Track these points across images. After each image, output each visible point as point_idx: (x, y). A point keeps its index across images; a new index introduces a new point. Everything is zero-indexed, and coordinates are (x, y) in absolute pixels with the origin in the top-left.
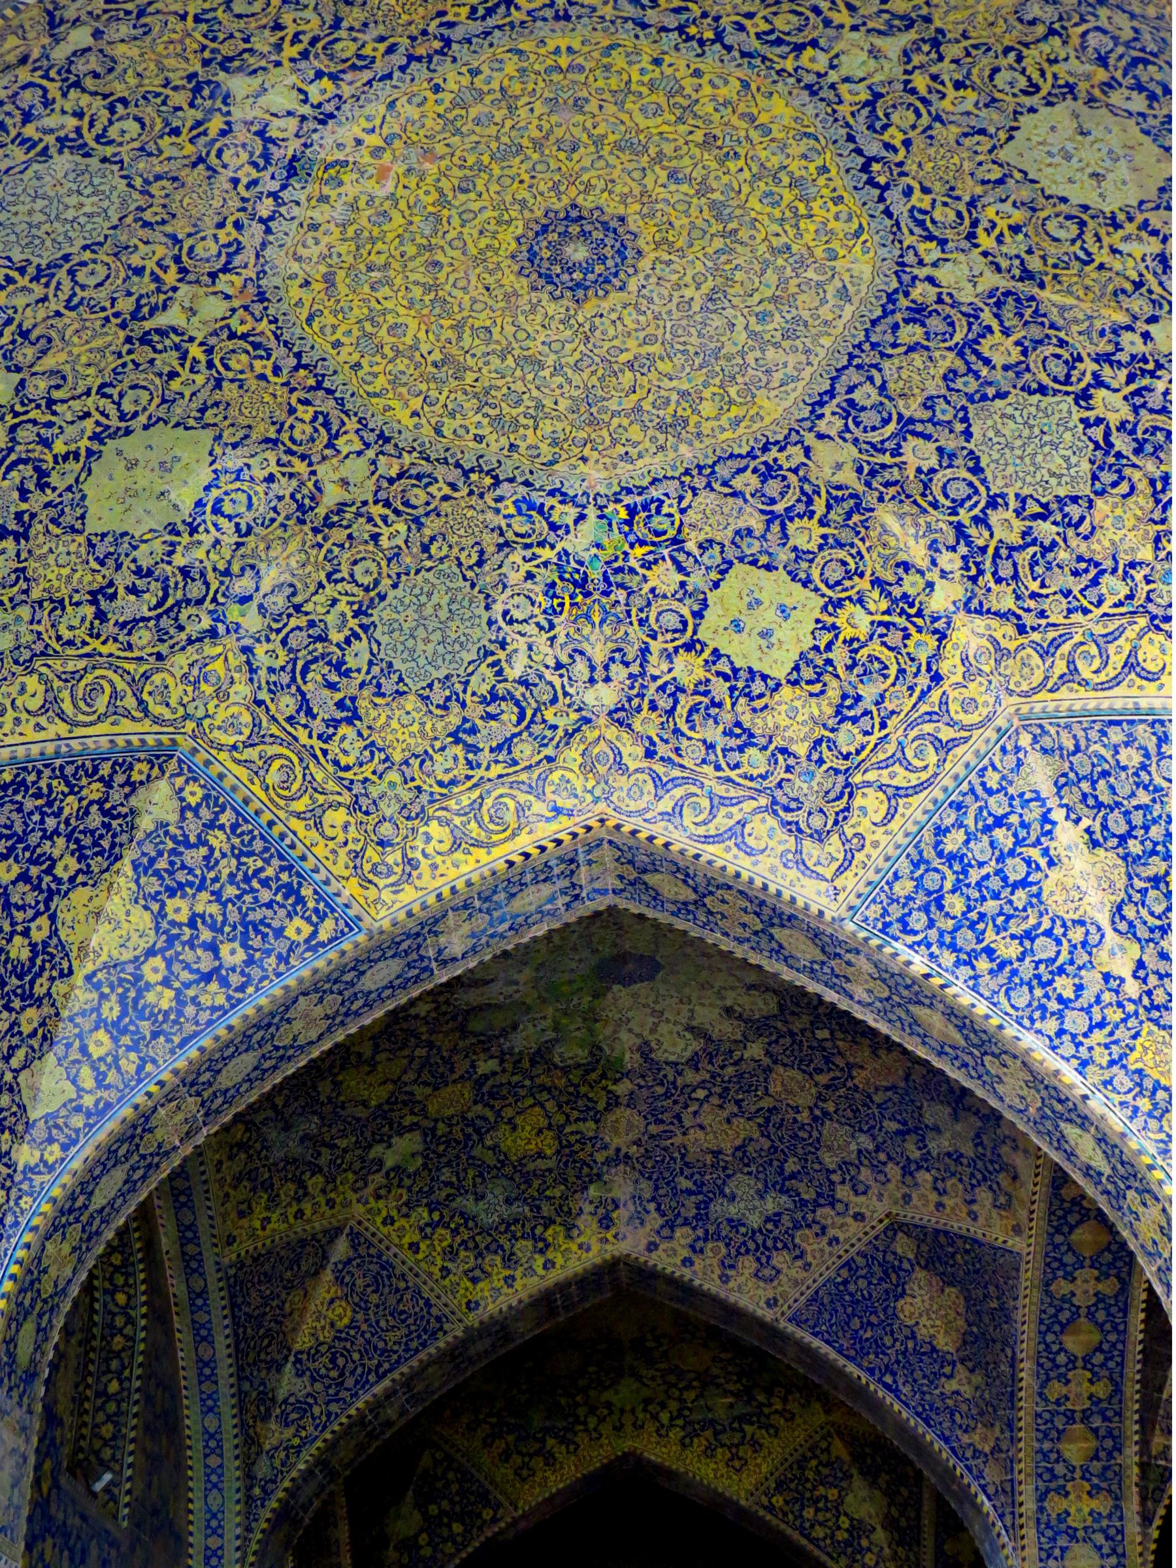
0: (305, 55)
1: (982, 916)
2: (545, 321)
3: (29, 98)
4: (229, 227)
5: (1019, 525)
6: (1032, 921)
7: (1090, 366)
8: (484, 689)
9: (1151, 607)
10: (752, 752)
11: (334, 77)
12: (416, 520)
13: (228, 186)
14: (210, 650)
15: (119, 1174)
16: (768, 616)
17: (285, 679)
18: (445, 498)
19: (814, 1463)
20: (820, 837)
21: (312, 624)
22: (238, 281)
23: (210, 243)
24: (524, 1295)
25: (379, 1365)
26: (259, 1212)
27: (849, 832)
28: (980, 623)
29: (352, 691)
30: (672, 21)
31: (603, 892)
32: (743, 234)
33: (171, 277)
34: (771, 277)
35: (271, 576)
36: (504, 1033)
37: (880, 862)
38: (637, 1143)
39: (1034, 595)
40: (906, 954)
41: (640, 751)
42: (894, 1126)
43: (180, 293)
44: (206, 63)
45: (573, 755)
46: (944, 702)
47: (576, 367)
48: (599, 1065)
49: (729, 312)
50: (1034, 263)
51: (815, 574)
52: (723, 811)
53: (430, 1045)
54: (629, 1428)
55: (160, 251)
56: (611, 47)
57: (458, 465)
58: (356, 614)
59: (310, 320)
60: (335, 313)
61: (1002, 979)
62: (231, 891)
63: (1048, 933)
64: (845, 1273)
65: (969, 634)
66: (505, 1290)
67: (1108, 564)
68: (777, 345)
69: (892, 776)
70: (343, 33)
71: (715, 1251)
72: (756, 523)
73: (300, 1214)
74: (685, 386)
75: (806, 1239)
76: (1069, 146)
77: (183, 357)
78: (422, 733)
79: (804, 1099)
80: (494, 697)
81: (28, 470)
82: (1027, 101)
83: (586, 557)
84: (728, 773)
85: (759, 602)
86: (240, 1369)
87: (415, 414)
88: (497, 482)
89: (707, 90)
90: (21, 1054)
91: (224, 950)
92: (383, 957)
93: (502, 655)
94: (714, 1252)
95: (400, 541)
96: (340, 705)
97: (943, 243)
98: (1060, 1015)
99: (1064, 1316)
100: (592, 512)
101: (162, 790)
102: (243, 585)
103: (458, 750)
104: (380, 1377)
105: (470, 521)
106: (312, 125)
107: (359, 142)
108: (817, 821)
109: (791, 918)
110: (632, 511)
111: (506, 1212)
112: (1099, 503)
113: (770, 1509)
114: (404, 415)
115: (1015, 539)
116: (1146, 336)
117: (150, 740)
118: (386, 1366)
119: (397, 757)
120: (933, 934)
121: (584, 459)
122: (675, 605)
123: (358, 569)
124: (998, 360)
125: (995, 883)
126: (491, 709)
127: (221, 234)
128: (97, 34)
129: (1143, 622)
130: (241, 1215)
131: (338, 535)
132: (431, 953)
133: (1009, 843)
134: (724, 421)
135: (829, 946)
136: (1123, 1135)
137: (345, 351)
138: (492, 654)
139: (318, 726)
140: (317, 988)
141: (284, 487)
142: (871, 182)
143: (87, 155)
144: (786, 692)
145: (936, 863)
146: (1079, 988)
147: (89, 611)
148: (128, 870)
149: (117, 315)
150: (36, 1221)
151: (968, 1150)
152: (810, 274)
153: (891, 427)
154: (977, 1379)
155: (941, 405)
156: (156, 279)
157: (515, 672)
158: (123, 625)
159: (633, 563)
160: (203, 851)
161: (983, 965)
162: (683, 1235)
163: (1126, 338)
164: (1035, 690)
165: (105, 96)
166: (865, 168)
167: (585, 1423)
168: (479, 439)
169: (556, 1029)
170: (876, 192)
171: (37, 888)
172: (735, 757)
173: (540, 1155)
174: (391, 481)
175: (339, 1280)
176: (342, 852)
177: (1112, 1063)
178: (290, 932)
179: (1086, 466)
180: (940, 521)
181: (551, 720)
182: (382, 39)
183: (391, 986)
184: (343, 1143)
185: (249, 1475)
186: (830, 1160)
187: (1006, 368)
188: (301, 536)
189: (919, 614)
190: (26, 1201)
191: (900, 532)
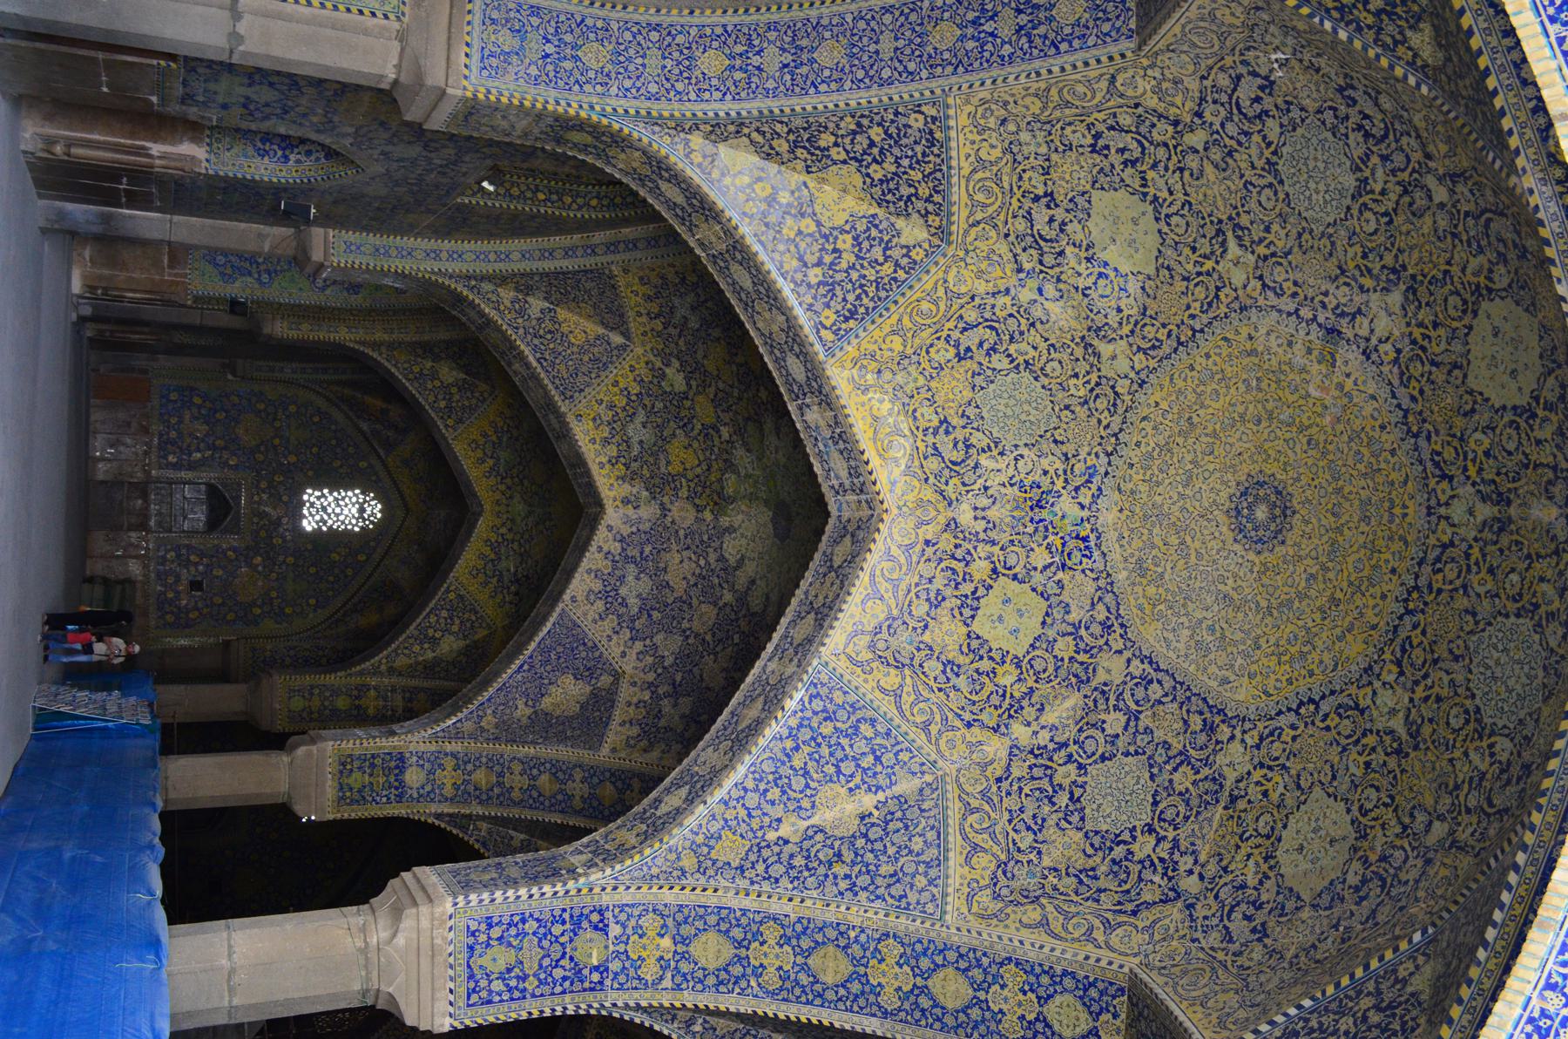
0: (1414, 342)
1: (819, 745)
2: (1217, 490)
3: (1399, 159)
4: (1294, 289)
5: (1066, 783)
6: (815, 776)
7: (1171, 834)
8: (973, 441)
9: (1012, 863)
10: (926, 606)
11: (1396, 361)
12: (1086, 402)
13: (1323, 289)
14: (1010, 267)
15: (680, 200)
16: (1012, 622)
17: (987, 315)
18: (1099, 421)
20: (872, 647)
21: (1022, 333)
22: (1255, 294)
23: (1284, 276)
24: (584, 449)
26: (642, 290)
27: (874, 665)
28: (1004, 754)
29: (977, 358)
30: (1422, 582)
31: (840, 510)
32: (1269, 620)
33: (1262, 250)
34: (1238, 636)
35: (1055, 309)
36: (745, 444)
37: (855, 683)
38: (673, 522)
39: (1020, 789)
40: (797, 696)
41: (929, 537)
42: (678, 678)
43: (1250, 256)
44: (1413, 277)
45: (928, 494)
46: (953, 729)
47: (1183, 509)
48: (721, 502)
49: (1216, 608)
50: (1241, 804)
51: (1037, 652)
52: (890, 587)
53: (740, 399)
55: (1280, 244)
56: (1406, 543)
57: (1121, 430)
58: (1026, 362)
59: (1225, 339)
60: (1229, 355)
61: (780, 755)
62: (855, 275)
63: (807, 786)
64: (590, 644)
65: (996, 748)
67: (1040, 837)
68: (1192, 637)
69: (908, 694)
70: (1427, 368)
71: (606, 567)
72: (1074, 617)
73: (639, 314)
74: (1167, 577)
75: (610, 622)
76: (1323, 833)
77: (1205, 257)
78: (948, 401)
79: (696, 625)
80: (968, 447)
81: (1137, 154)
82: (1355, 808)
83: (1056, 509)
84: (914, 591)
85: (1021, 616)
86: (547, 275)
87: (1157, 404)
88: (1108, 455)
89: (1371, 602)
90: (760, 139)
91: (818, 270)
92: (807, 370)
93: (995, 452)
94: (604, 565)
95: (1073, 391)
96: (968, 349)
97: (1258, 747)
98: (756, 790)
99: (560, 775)
100: (1085, 513)
101: (921, 234)
102: (1050, 290)
103: (936, 423)
104: (538, 360)
105: (1083, 437)
106: (1363, 345)
107: (1348, 375)
108: (881, 645)
109: (821, 626)
110: (1085, 539)
111: (635, 439)
112: (1081, 834)
113: (448, 591)
114: (1157, 397)
115: (1057, 779)
116: (1191, 872)
117: (954, 228)
119: (933, 384)
120: (809, 714)
121: (1121, 511)
122: (1022, 563)
123: (1055, 364)
124: (1177, 777)
125: (839, 754)
126: (960, 445)
127: (1290, 284)
128: (1442, 206)
129: (1003, 857)
130: (641, 279)
131: (1079, 352)
132: (808, 401)
133: (864, 765)
134: (1141, 600)
135: (804, 648)
136: (681, 825)
137: (1203, 361)
138: (995, 446)
139: (956, 335)
140: (791, 327)
141: (1113, 319)
142: (1301, 704)
143: (1353, 197)
144: (964, 630)
145: (853, 718)
146: (773, 803)
147: (1040, 192)
148: (872, 211)
149: (1238, 214)
150: (655, 146)
151: (663, 723)
152: (1240, 661)
153: (1134, 707)
154: (525, 721)
155: (1147, 738)
156: (1261, 241)
157: (984, 461)
158: (1029, 213)
159: (1051, 538)
160: (881, 259)
161: (789, 744)
162: (616, 547)
163: (1190, 860)
164: (960, 786)
165: (1395, 210)
166: (1311, 701)
168: (1138, 444)
169: (748, 476)
170: (1294, 707)
171: (865, 153)
172: (923, 596)
173: (668, 463)
174: (1113, 387)
175: (598, 338)
176: (875, 347)
177: (726, 821)
178: (827, 312)
179: (1105, 827)
180: (1070, 733)
181: (951, 482)
182: (1421, 392)
183: (788, 374)
184: (681, 342)
185: (483, 278)
186: (659, 638)
187: (1171, 781)
188: (1080, 329)
189: (1010, 716)
190: (667, 139)
191: (1064, 709)
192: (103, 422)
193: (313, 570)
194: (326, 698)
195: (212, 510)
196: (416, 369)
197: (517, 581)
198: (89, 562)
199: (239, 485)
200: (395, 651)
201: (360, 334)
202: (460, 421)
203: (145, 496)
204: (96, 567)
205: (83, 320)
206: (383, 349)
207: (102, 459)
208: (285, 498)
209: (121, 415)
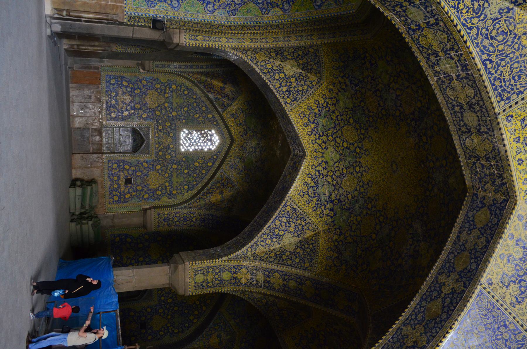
19: (303, 224)
25: (491, 62)
54: (315, 154)
66: (513, 137)
113: (285, 205)
118: (489, 66)
167: (319, 139)
192: (77, 96)
193: (186, 171)
194: (217, 274)
195: (134, 140)
196: (269, 66)
197: (332, 201)
198: (74, 171)
199: (148, 128)
200: (256, 242)
201: (234, 43)
202: (295, 100)
203: (100, 134)
204: (77, 173)
205: (61, 35)
206: (249, 53)
207: (77, 116)
208: (171, 135)
209: (87, 92)
